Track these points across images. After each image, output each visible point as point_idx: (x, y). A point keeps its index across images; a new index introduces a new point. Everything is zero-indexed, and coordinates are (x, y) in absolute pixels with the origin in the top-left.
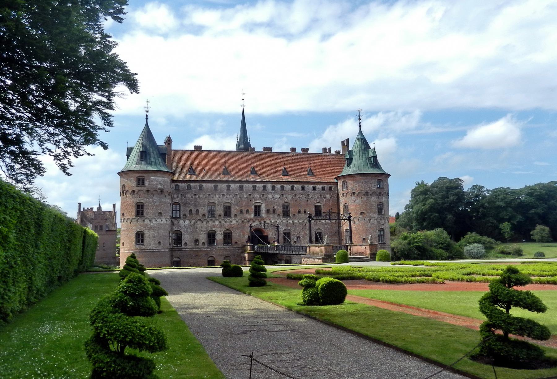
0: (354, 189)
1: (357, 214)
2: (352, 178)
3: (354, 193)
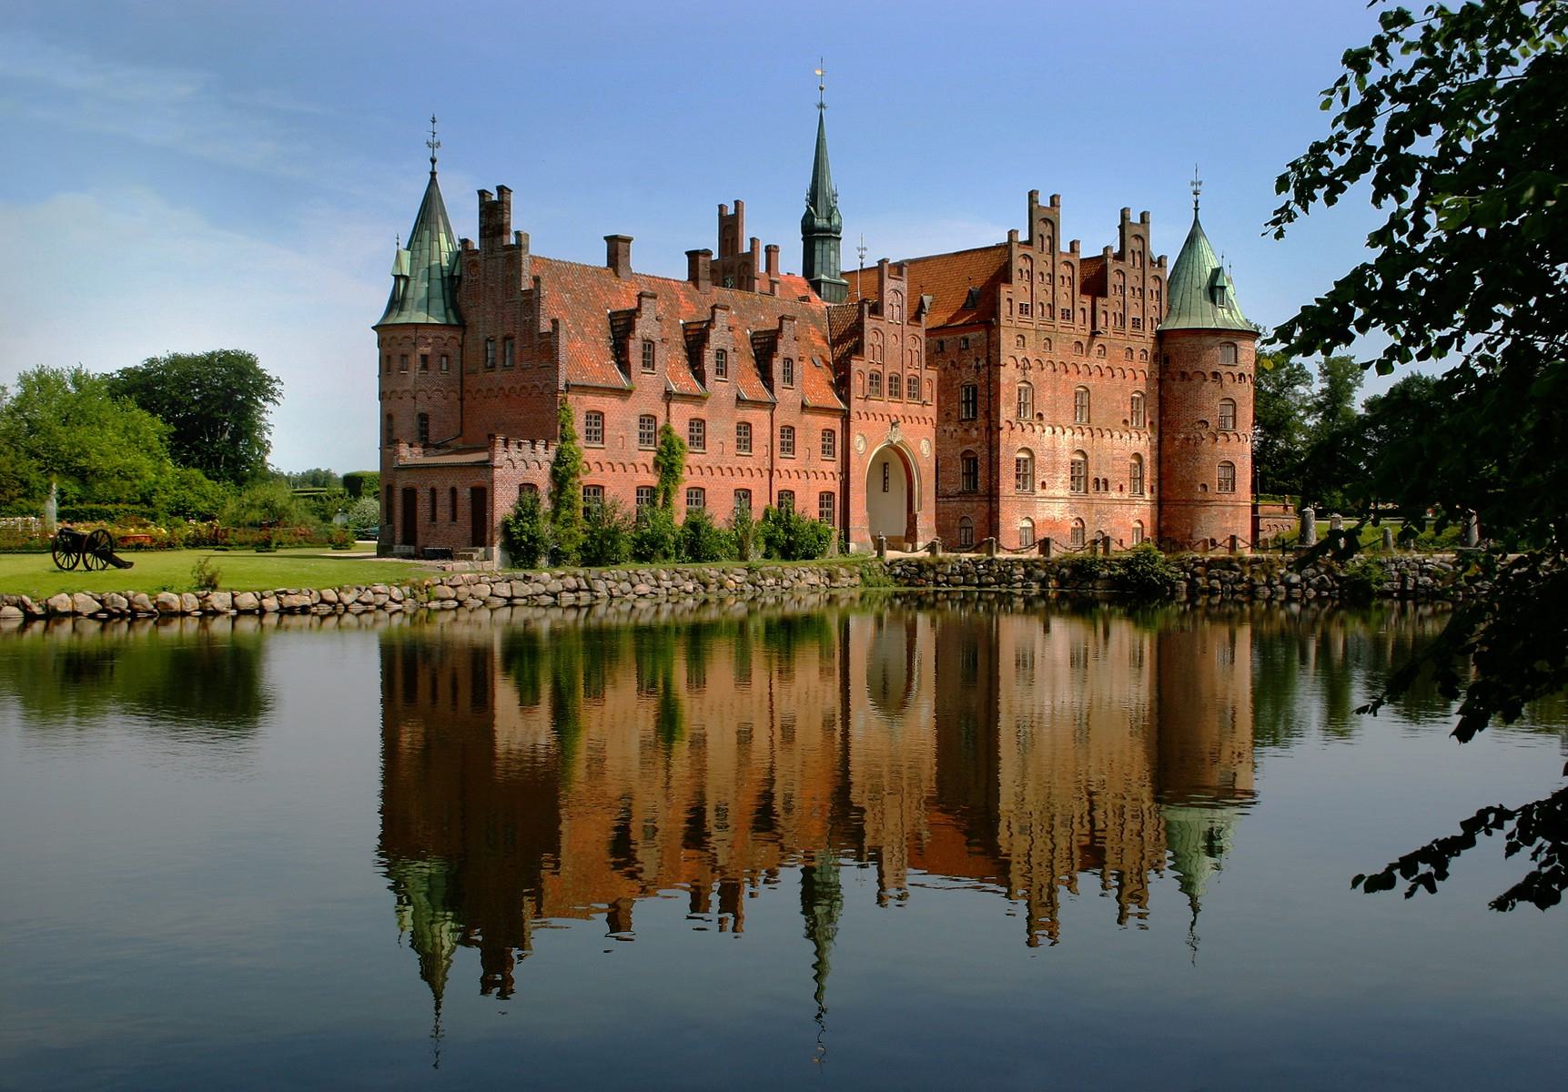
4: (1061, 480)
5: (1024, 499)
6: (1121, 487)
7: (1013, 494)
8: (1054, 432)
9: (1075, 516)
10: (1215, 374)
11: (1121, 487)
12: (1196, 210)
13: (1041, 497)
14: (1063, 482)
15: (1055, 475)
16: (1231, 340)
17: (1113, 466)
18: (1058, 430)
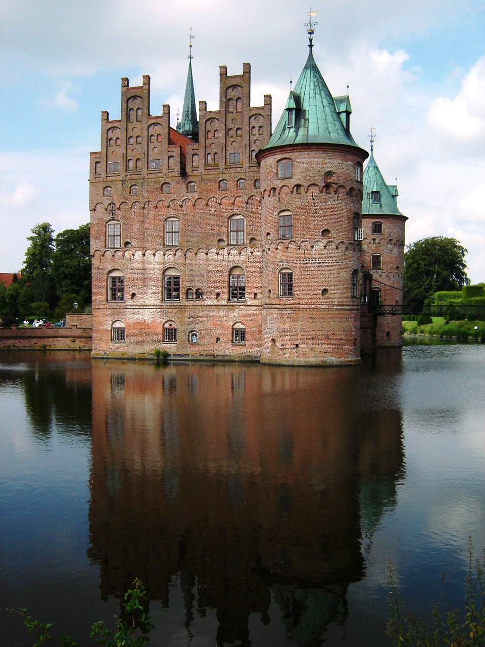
0: (391, 234)
1: (394, 268)
2: (391, 220)
3: (391, 240)
4: (151, 291)
5: (115, 307)
6: (218, 295)
7: (104, 303)
8: (144, 255)
9: (166, 319)
10: (274, 189)
11: (218, 295)
12: (311, 46)
13: (131, 305)
14: (153, 293)
15: (145, 288)
16: (287, 155)
17: (208, 278)
18: (147, 253)
